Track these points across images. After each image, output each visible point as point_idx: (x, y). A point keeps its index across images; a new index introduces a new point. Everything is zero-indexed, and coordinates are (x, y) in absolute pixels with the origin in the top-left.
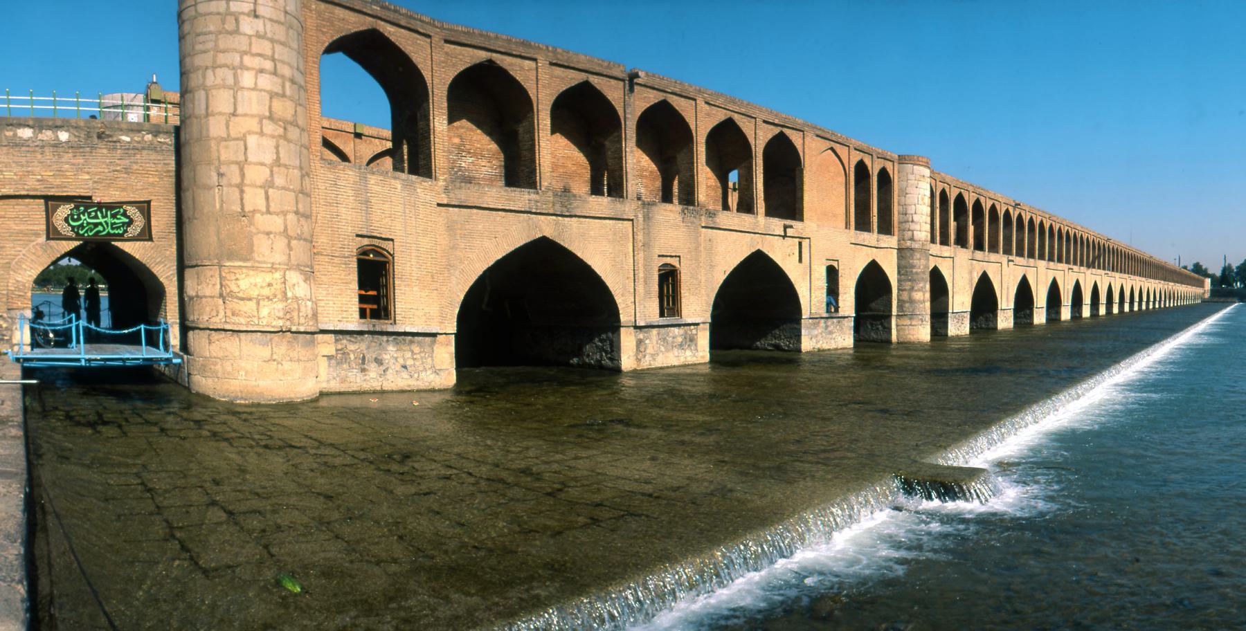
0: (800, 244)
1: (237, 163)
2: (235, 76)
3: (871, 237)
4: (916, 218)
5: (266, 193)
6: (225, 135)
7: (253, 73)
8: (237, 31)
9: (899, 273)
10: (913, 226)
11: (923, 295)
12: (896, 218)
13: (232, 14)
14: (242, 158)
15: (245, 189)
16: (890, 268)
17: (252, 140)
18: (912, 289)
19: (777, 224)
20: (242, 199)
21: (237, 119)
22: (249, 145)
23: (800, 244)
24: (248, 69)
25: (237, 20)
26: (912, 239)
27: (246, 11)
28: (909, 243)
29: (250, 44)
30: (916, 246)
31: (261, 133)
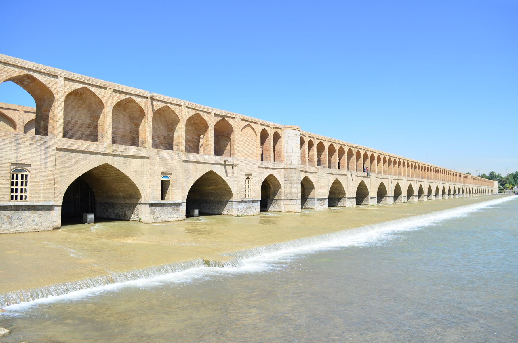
0: (232, 167)
3: (270, 164)
4: (292, 154)
9: (285, 180)
10: (291, 158)
11: (297, 190)
16: (279, 176)
18: (291, 187)
19: (220, 159)
23: (232, 167)
26: (291, 164)
28: (289, 166)
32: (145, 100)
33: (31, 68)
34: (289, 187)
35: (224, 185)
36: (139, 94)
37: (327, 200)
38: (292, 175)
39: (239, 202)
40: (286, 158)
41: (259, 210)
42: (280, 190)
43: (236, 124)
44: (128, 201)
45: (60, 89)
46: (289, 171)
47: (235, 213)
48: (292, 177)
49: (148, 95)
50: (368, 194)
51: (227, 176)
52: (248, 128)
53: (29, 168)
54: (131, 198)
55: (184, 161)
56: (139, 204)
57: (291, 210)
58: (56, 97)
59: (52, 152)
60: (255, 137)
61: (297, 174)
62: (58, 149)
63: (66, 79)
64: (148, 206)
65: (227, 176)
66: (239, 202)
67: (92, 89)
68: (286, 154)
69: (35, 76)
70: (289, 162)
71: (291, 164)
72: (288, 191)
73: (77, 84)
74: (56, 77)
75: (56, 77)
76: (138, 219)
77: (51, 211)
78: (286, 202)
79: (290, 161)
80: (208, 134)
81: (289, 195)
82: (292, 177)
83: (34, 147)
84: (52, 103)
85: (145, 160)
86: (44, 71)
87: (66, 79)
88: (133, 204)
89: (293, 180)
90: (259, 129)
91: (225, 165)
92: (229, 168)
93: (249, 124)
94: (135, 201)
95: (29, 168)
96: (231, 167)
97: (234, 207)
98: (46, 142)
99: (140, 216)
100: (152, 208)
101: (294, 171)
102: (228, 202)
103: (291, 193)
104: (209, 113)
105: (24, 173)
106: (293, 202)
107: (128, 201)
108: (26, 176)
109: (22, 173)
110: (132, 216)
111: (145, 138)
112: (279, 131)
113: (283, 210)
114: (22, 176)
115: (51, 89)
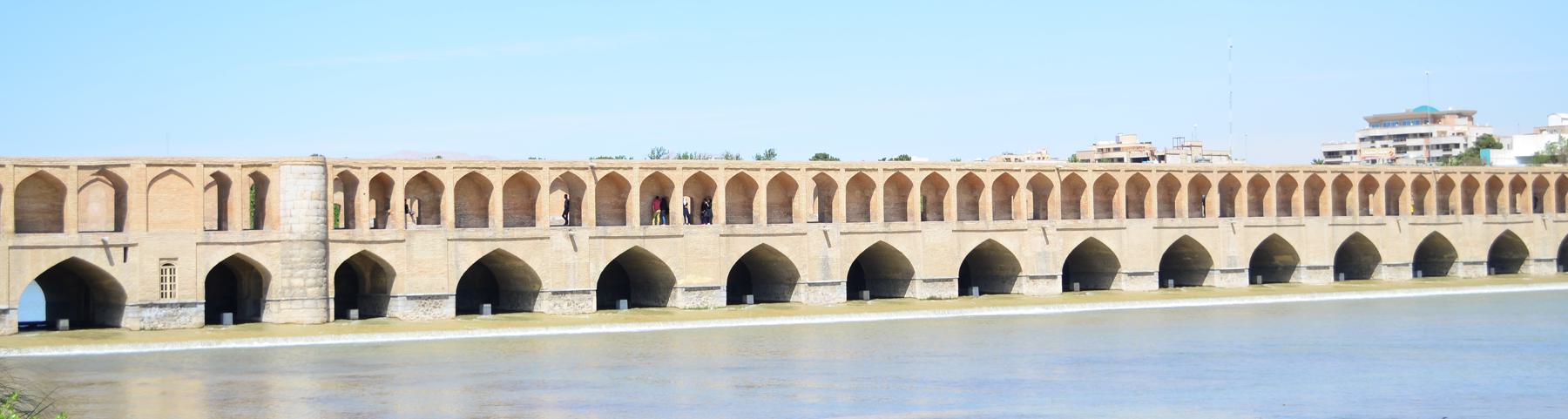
0: (126, 250)
23: (126, 250)
28: (287, 236)
30: (292, 237)
37: (453, 300)
40: (283, 221)
41: (202, 320)
47: (137, 325)
50: (674, 281)
51: (112, 263)
52: (172, 176)
61: (305, 251)
65: (112, 263)
68: (282, 213)
70: (287, 228)
72: (285, 283)
78: (284, 305)
90: (203, 176)
91: (106, 246)
93: (170, 171)
96: (121, 250)
101: (297, 245)
103: (291, 287)
106: (294, 305)
112: (264, 171)
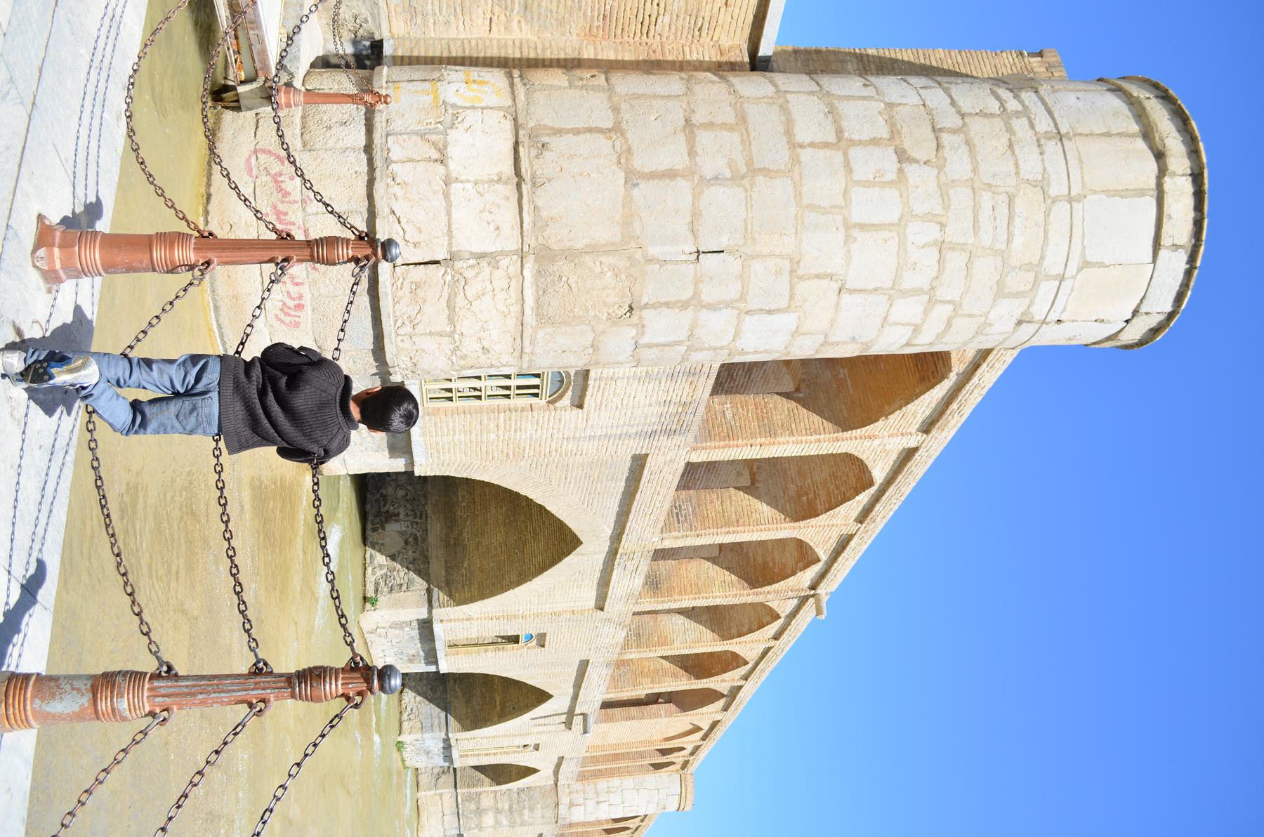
1: (743, 297)
2: (918, 292)
5: (679, 343)
6: (800, 272)
7: (918, 321)
8: (1001, 292)
12: (602, 784)
13: (1036, 284)
14: (753, 304)
15: (688, 314)
17: (789, 320)
18: (498, 811)
20: (667, 305)
21: (833, 295)
22: (775, 318)
24: (926, 312)
25: (1017, 295)
26: (571, 805)
27: (1033, 309)
28: (564, 800)
29: (970, 316)
31: (796, 333)
32: (807, 584)
33: (975, 380)
34: (500, 806)
35: (503, 706)
36: (829, 576)
38: (538, 812)
39: (447, 741)
42: (487, 780)
43: (704, 716)
44: (436, 529)
45: (877, 442)
46: (551, 801)
48: (532, 810)
49: (821, 590)
53: (566, 401)
54: (447, 545)
55: (584, 665)
56: (429, 591)
57: (423, 818)
58: (848, 434)
59: (637, 447)
60: (660, 737)
62: (639, 463)
63: (909, 454)
64: (424, 615)
66: (447, 741)
67: (864, 498)
69: (938, 387)
70: (578, 798)
71: (571, 805)
72: (487, 801)
73: (887, 469)
74: (927, 427)
75: (927, 427)
76: (370, 593)
77: (386, 452)
79: (581, 801)
80: (675, 676)
81: (473, 807)
82: (532, 810)
83: (656, 410)
84: (820, 413)
85: (592, 604)
86: (954, 406)
87: (909, 454)
88: (426, 559)
89: (521, 815)
92: (563, 718)
94: (437, 567)
95: (566, 401)
97: (427, 735)
98: (670, 433)
99: (382, 599)
100: (415, 624)
102: (446, 708)
103: (479, 812)
104: (746, 678)
105: (546, 390)
107: (436, 529)
108: (536, 395)
109: (546, 390)
110: (381, 559)
111: (670, 590)
113: (421, 794)
114: (537, 387)
115: (880, 423)
